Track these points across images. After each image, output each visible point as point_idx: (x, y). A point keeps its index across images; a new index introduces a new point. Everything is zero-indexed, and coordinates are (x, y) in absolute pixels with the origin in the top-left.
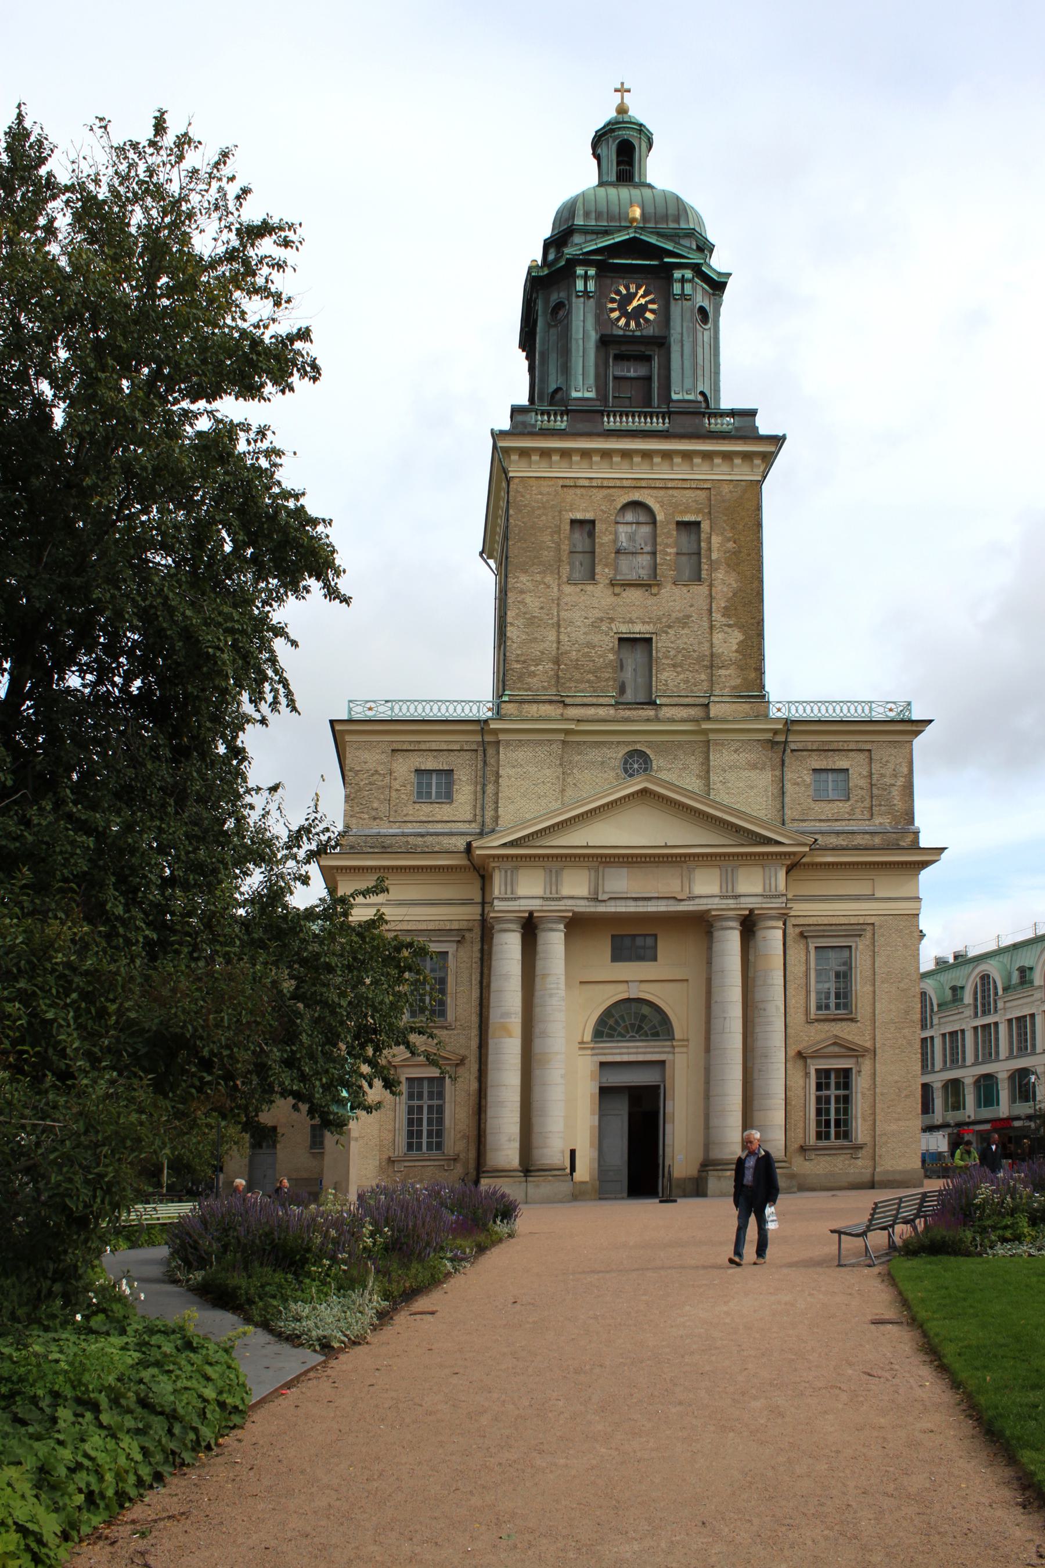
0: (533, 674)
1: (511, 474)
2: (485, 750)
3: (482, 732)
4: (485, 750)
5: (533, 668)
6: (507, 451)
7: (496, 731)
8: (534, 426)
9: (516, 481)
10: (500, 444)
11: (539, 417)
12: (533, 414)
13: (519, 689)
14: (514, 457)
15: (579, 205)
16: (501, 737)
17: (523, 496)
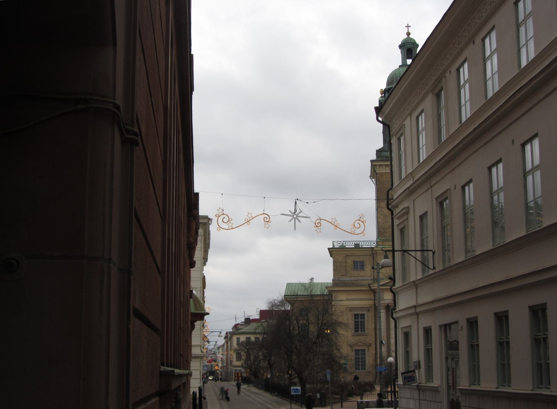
0: (386, 232)
1: (377, 172)
2: (373, 256)
3: (372, 250)
4: (373, 256)
5: (386, 231)
6: (376, 165)
7: (376, 250)
8: (383, 156)
9: (379, 174)
10: (374, 164)
11: (385, 153)
12: (383, 152)
13: (383, 237)
14: (378, 167)
15: (395, 79)
16: (378, 252)
17: (381, 178)
